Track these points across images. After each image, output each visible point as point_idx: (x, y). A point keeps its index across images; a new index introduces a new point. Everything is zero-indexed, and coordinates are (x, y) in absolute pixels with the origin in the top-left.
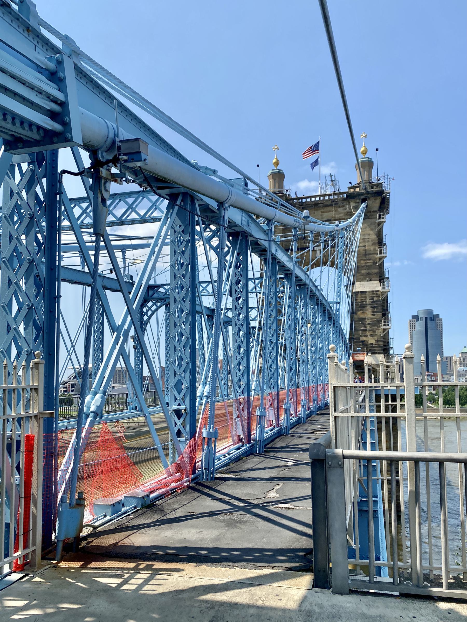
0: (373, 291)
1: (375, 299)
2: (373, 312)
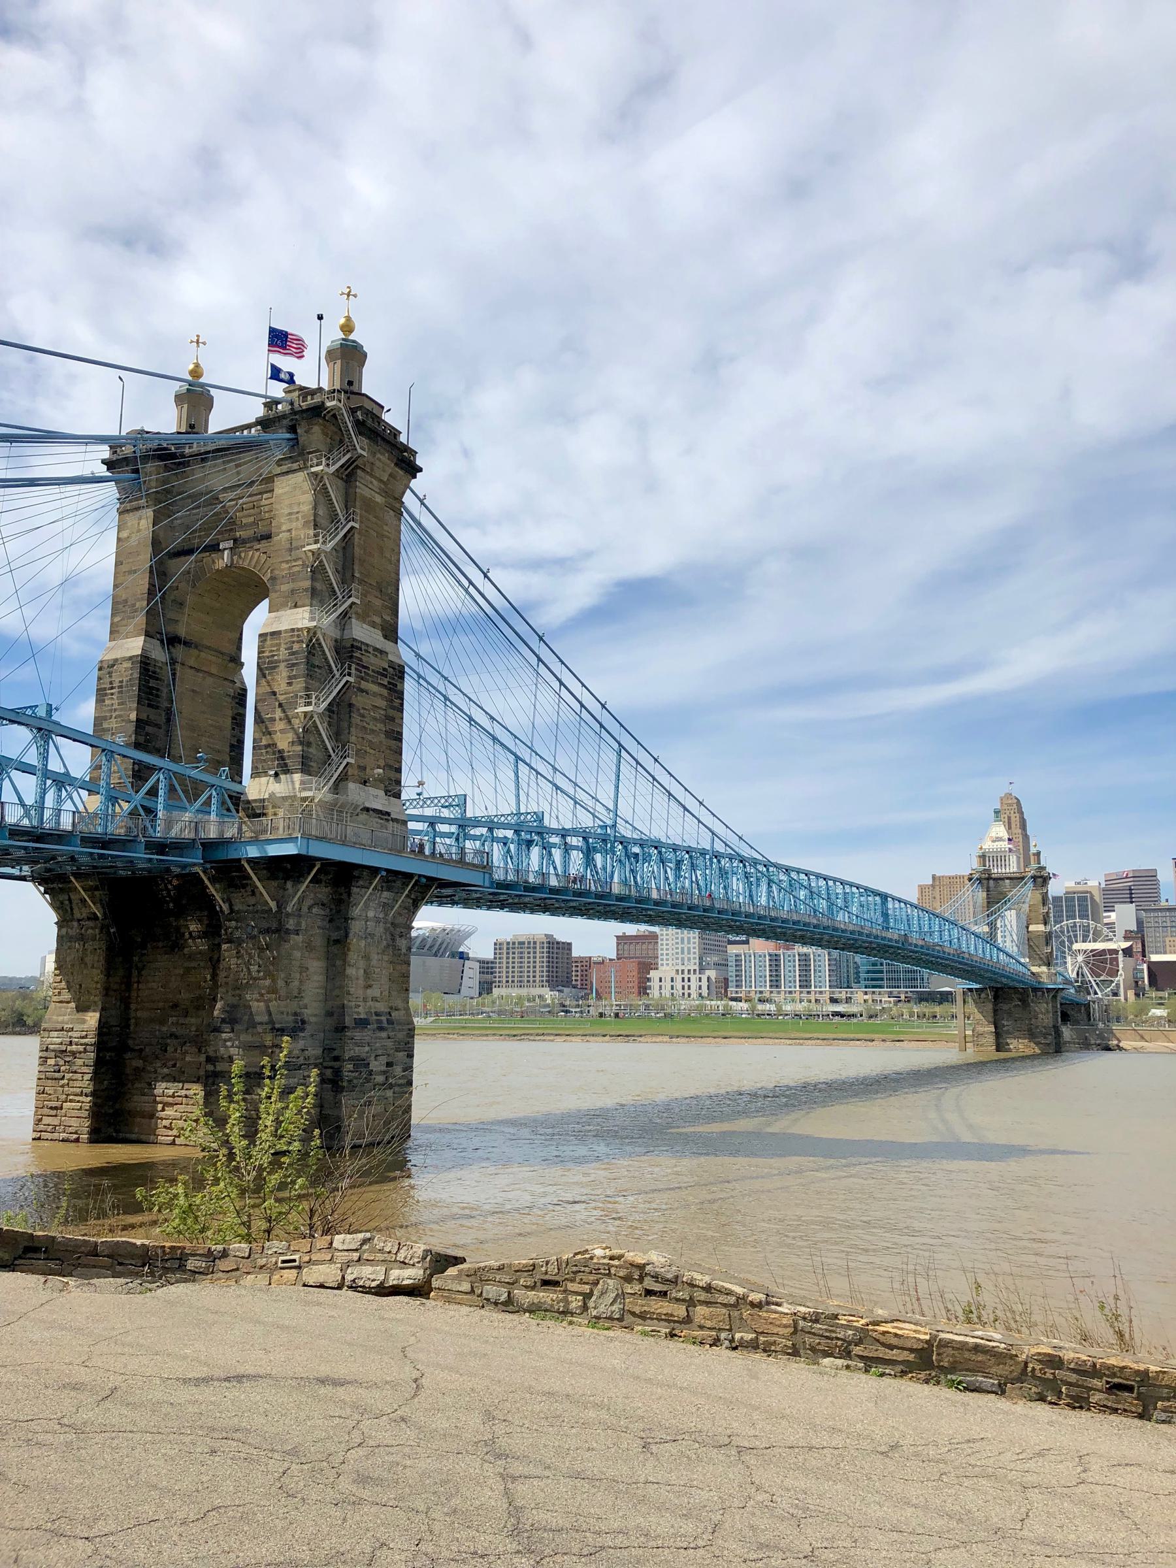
0: (293, 630)
1: (296, 647)
2: (289, 677)
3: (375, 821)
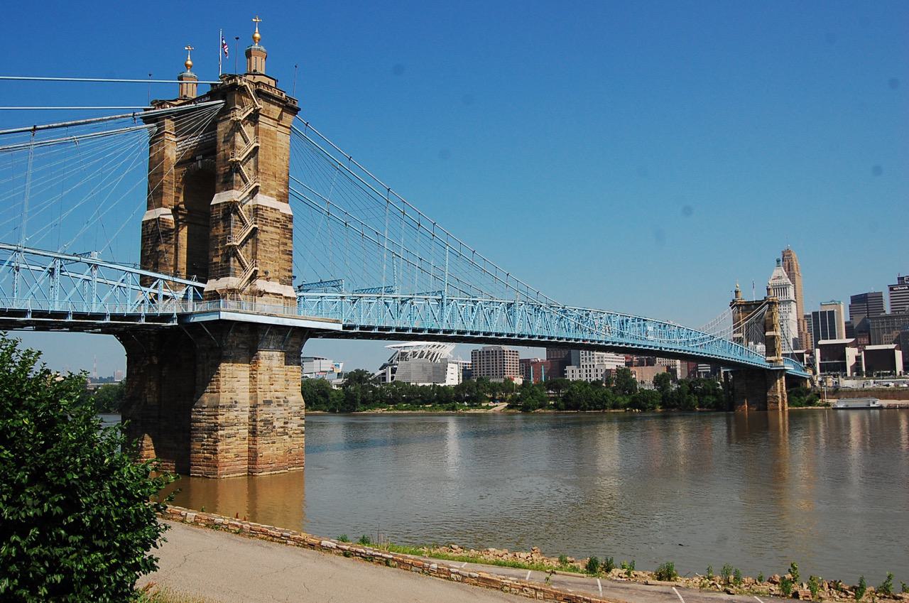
3: (273, 298)
